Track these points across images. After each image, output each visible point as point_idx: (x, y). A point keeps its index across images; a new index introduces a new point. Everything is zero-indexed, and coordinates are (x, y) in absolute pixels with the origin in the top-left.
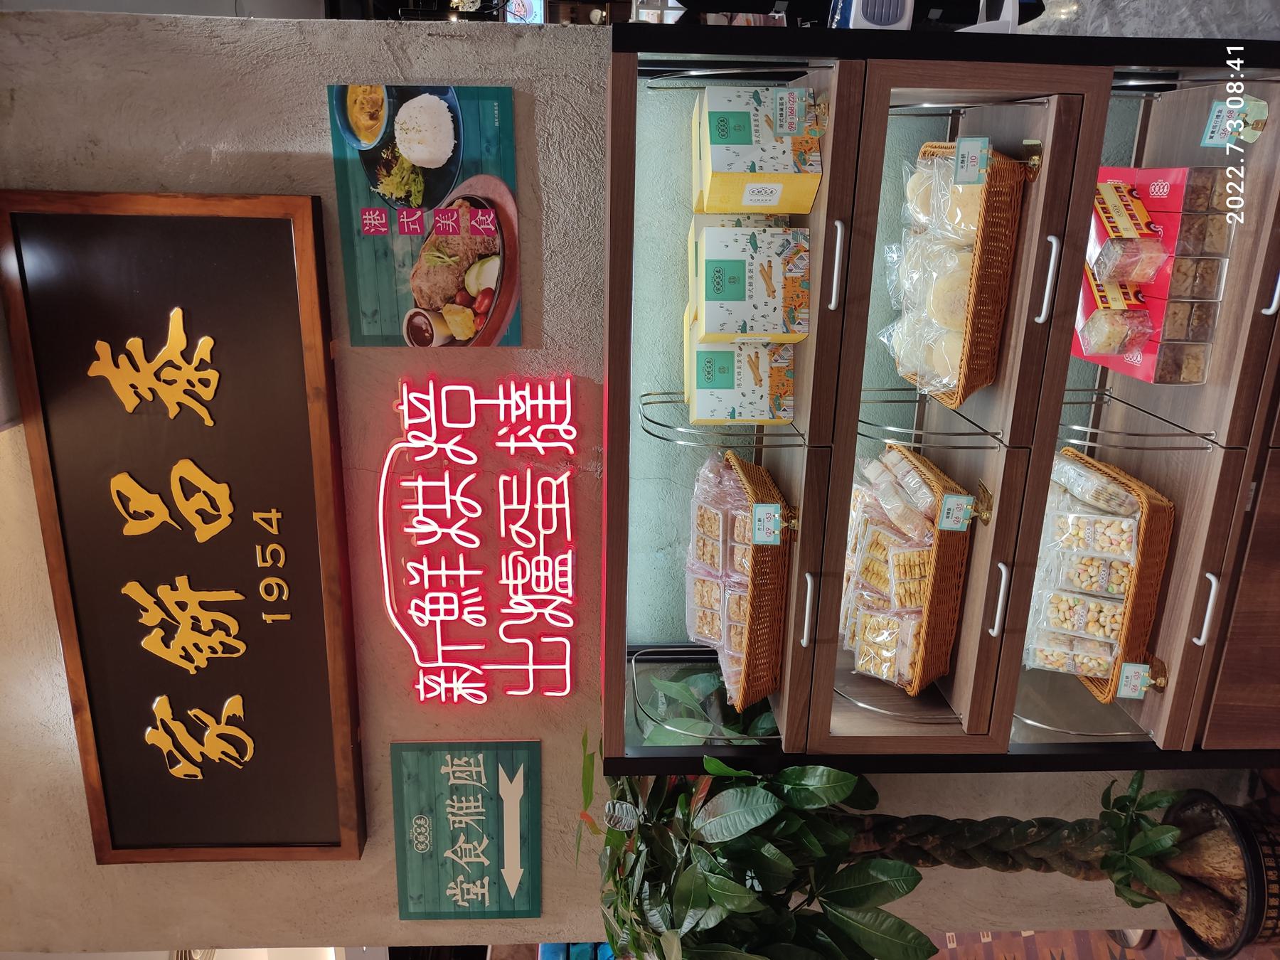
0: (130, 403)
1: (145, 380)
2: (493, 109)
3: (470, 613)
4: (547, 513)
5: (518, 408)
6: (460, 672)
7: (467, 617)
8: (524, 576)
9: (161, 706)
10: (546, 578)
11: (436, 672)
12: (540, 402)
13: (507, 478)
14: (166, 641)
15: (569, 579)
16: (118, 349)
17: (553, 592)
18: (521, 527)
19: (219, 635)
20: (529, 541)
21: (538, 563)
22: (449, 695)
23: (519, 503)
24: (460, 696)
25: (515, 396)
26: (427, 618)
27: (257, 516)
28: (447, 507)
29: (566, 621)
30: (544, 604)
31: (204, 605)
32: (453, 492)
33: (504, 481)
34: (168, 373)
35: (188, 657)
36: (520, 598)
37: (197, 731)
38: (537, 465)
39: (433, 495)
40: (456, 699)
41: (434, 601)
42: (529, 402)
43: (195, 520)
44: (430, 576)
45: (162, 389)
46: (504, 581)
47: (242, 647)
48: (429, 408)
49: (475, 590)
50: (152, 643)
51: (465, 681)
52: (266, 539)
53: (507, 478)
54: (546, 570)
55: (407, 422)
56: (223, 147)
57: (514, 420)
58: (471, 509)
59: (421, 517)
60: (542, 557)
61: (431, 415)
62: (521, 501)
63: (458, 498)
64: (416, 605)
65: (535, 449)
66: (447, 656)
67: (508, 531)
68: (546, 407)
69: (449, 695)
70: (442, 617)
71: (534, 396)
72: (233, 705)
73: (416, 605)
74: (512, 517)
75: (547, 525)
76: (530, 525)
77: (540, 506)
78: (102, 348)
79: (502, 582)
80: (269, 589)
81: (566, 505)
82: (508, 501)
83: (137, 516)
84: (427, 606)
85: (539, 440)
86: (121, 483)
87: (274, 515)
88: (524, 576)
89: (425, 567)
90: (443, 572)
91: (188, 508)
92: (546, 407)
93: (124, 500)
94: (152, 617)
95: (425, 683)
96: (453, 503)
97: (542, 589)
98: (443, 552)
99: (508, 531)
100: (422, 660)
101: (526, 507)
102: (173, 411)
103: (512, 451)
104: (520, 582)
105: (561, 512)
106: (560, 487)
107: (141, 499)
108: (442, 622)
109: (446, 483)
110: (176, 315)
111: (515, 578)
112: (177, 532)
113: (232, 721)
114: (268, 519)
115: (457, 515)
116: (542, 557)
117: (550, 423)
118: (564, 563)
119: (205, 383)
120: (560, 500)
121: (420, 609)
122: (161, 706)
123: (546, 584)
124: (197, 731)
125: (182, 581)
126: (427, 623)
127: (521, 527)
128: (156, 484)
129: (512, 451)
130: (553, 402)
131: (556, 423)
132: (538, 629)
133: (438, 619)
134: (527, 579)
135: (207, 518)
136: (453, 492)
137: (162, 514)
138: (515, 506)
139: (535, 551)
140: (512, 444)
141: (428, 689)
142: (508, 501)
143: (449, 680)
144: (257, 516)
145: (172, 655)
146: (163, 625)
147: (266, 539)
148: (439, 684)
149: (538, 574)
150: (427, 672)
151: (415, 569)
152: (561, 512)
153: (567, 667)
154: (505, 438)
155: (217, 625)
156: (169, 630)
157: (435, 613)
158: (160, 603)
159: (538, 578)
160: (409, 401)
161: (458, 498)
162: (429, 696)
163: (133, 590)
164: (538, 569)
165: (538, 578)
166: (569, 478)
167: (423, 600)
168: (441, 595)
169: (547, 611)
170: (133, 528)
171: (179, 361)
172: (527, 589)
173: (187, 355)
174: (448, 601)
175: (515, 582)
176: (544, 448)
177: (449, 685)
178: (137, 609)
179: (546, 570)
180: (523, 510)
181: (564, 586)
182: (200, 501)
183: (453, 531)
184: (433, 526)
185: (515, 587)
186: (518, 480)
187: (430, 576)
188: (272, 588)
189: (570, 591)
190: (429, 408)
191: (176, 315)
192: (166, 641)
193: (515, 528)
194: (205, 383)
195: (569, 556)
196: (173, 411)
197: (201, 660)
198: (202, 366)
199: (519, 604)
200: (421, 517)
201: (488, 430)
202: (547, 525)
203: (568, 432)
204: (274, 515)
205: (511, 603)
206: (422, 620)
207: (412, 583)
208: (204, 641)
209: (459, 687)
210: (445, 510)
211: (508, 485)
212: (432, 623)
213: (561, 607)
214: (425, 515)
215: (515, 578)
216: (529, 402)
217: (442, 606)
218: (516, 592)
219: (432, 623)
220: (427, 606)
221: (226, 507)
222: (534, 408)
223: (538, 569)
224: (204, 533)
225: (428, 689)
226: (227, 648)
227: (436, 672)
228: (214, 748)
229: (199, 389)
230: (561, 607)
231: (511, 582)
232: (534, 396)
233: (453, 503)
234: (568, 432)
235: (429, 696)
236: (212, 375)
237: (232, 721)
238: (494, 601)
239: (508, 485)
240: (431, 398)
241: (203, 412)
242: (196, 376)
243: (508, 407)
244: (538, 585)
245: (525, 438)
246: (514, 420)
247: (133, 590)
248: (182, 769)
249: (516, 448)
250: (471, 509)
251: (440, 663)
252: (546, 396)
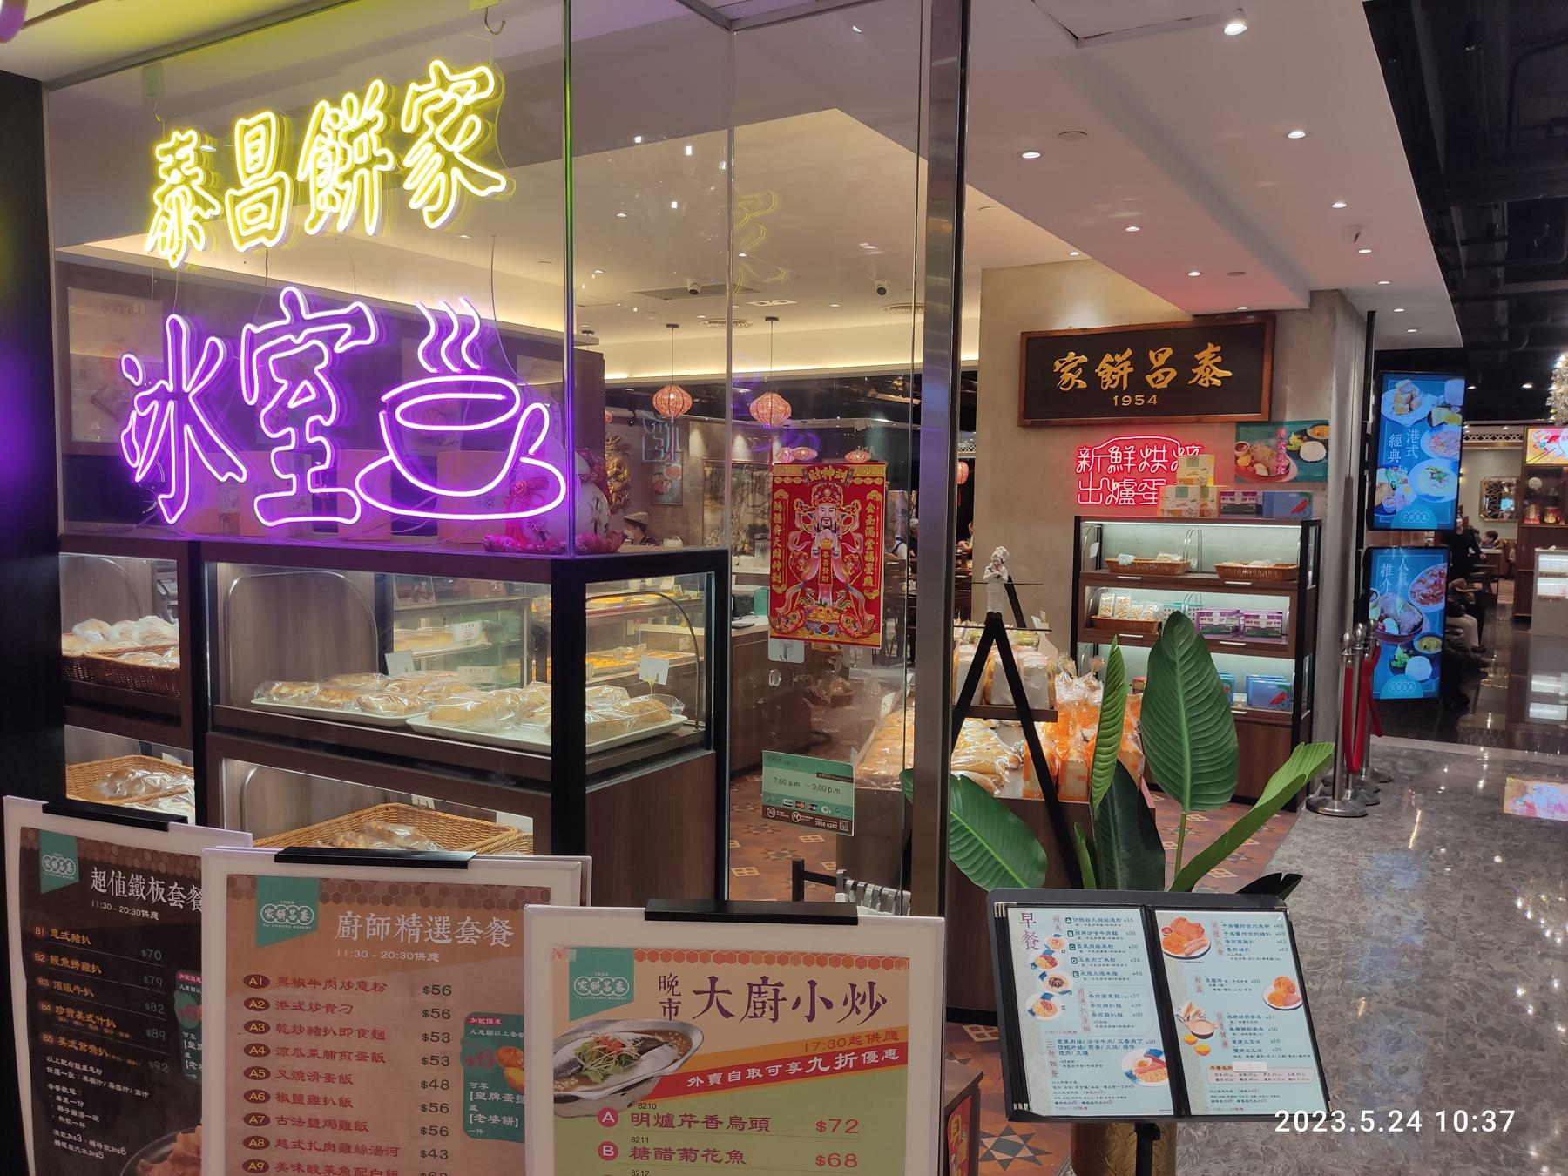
0: (1198, 357)
1: (1206, 362)
2: (1320, 475)
4: (1151, 496)
6: (1090, 463)
7: (1111, 466)
9: (1083, 359)
11: (1090, 455)
14: (1109, 363)
16: (1217, 354)
19: (1110, 381)
26: (1112, 452)
27: (1155, 396)
28: (1155, 460)
30: (1115, 493)
31: (1122, 377)
34: (1208, 370)
35: (1102, 370)
36: (1118, 485)
37: (1073, 371)
39: (1159, 456)
41: (1119, 455)
43: (1154, 376)
45: (1203, 367)
47: (1105, 389)
50: (1108, 357)
52: (1146, 399)
56: (1289, 389)
60: (1134, 494)
63: (1158, 465)
66: (1096, 459)
72: (1082, 384)
74: (1150, 484)
75: (1146, 496)
76: (1147, 490)
78: (1218, 349)
80: (1127, 399)
83: (1156, 356)
84: (1116, 453)
86: (1169, 351)
87: (1155, 402)
89: (1132, 452)
90: (1130, 458)
91: (1159, 373)
93: (1163, 352)
94: (1118, 358)
98: (1137, 458)
102: (1194, 371)
107: (1163, 358)
109: (1164, 461)
110: (1229, 374)
112: (1150, 369)
113: (1076, 384)
114: (1153, 400)
115: (1152, 464)
116: (1134, 494)
119: (1204, 382)
122: (1083, 359)
124: (1073, 371)
125: (1131, 369)
128: (1167, 364)
132: (1106, 492)
135: (1155, 380)
137: (1156, 364)
139: (1136, 491)
141: (1083, 452)
144: (1155, 396)
145: (1103, 364)
146: (1115, 362)
147: (1146, 399)
150: (1090, 452)
155: (1114, 381)
156: (1113, 364)
157: (1114, 455)
158: (1123, 361)
163: (1129, 352)
168: (1120, 458)
169: (1112, 495)
170: (1152, 354)
171: (1212, 374)
172: (1121, 488)
173: (1214, 377)
178: (1122, 353)
182: (1161, 377)
183: (1145, 463)
188: (1127, 401)
191: (1229, 374)
192: (1109, 363)
193: (1146, 485)
194: (1204, 382)
196: (1194, 371)
197: (1100, 374)
198: (1210, 382)
199: (1116, 485)
202: (1146, 496)
204: (1155, 402)
208: (1108, 376)
209: (1084, 463)
213: (1114, 500)
217: (1116, 457)
220: (1116, 453)
221: (1159, 386)
224: (1149, 378)
225: (1083, 452)
226: (1105, 384)
227: (1090, 455)
228: (1066, 377)
229: (1202, 380)
230: (1114, 500)
231: (1124, 482)
236: (1207, 385)
237: (1076, 384)
238: (1115, 476)
241: (1193, 381)
242: (1207, 379)
247: (1129, 352)
248: (1057, 363)
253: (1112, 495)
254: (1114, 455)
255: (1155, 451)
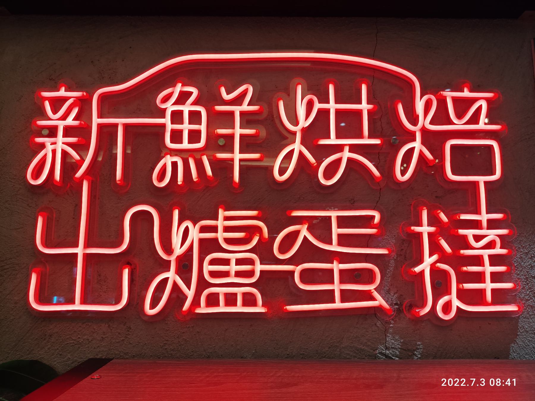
3: (175, 165)
5: (477, 238)
7: (168, 160)
8: (228, 241)
10: (226, 274)
12: (489, 269)
13: (377, 220)
15: (222, 309)
17: (203, 284)
18: (305, 237)
20: (283, 249)
21: (251, 262)
22: (45, 132)
23: (340, 236)
24: (43, 146)
25: (492, 234)
26: (170, 107)
28: (333, 140)
29: (154, 304)
32: (353, 148)
33: (373, 217)
36: (195, 234)
38: (392, 261)
40: (39, 140)
41: (195, 117)
42: (486, 253)
44: (232, 113)
46: (222, 213)
48: (467, 123)
49: (209, 172)
51: (65, 154)
53: (377, 220)
54: (238, 274)
55: (449, 94)
57: (462, 232)
58: (330, 172)
59: (317, 106)
61: (459, 125)
62: (343, 240)
64: (191, 93)
65: (421, 261)
67: (300, 220)
68: (479, 277)
69: (45, 132)
70: (170, 126)
71: (495, 260)
73: (191, 93)
77: (336, 267)
79: (221, 211)
81: (338, 305)
82: (343, 222)
84: (186, 109)
85: (433, 266)
88: (228, 241)
89: (245, 107)
92: (479, 277)
95: (66, 99)
96: (339, 148)
97: (207, 268)
99: (300, 220)
100: (103, 98)
101: (334, 247)
103: (418, 229)
104: (221, 235)
105: (329, 296)
106: (368, 296)
108: (163, 126)
111: (227, 229)
117: (458, 283)
118: (249, 300)
120: (346, 296)
121: (183, 98)
123: (213, 274)
126: (163, 106)
127: (305, 237)
129: (418, 229)
130: (489, 286)
131: (459, 290)
133: (167, 120)
134: (224, 246)
136: (353, 148)
138: (335, 231)
140: (425, 229)
141: (57, 103)
142: (343, 222)
143: (68, 131)
148: (64, 118)
149: (233, 262)
151: (244, 94)
152: (329, 296)
153: (77, 306)
154: (433, 221)
157: (177, 117)
159: (227, 262)
160: (476, 100)
161: (346, 154)
162: (47, 104)
164: (239, 262)
165: (227, 262)
166: (380, 308)
167: (194, 103)
168: (203, 128)
169: (171, 275)
174: (194, 136)
175: (220, 229)
176: (422, 272)
177: (60, 132)
179: (238, 274)
180: (330, 243)
181: (213, 300)
183: (297, 146)
184: (304, 123)
185: (214, 229)
186: (370, 235)
187: (232, 113)
189: (203, 310)
190: (467, 123)
193: (304, 232)
195: (259, 309)
200: (317, 106)
201: (436, 197)
203: (447, 307)
205: (188, 223)
206: (166, 99)
207: (223, 90)
210: (329, 137)
211: (367, 221)
212: (162, 113)
214: (320, 111)
215: (227, 229)
216: (486, 253)
217: (186, 127)
218: (203, 229)
219: (162, 113)
220: (186, 109)
222: (478, 260)
223: (239, 262)
225: (57, 103)
231: (220, 223)
232: (495, 260)
233: (339, 148)
234: (447, 307)
235: (47, 104)
239: (367, 221)
240: (483, 124)
243: (477, 225)
244: (213, 262)
245: (435, 248)
246: (462, 232)
249: (420, 234)
250: (330, 172)
251: (96, 121)
252: (496, 277)
253: (171, 275)
254: (177, 117)
255: (332, 106)
